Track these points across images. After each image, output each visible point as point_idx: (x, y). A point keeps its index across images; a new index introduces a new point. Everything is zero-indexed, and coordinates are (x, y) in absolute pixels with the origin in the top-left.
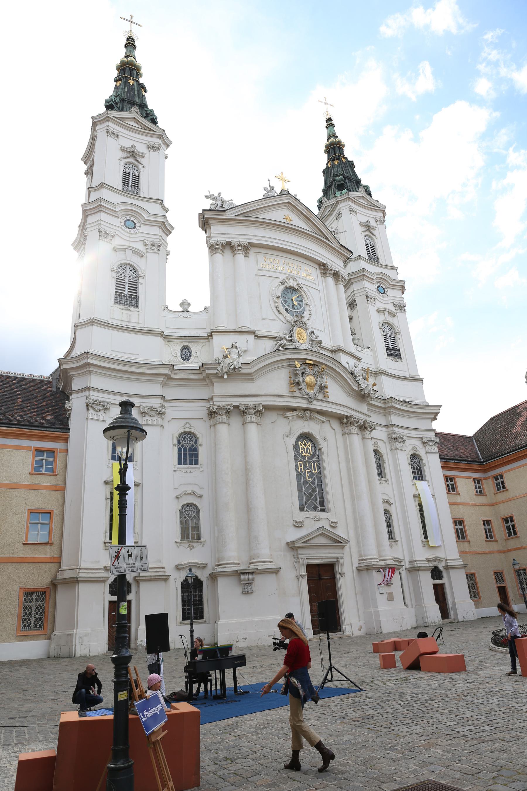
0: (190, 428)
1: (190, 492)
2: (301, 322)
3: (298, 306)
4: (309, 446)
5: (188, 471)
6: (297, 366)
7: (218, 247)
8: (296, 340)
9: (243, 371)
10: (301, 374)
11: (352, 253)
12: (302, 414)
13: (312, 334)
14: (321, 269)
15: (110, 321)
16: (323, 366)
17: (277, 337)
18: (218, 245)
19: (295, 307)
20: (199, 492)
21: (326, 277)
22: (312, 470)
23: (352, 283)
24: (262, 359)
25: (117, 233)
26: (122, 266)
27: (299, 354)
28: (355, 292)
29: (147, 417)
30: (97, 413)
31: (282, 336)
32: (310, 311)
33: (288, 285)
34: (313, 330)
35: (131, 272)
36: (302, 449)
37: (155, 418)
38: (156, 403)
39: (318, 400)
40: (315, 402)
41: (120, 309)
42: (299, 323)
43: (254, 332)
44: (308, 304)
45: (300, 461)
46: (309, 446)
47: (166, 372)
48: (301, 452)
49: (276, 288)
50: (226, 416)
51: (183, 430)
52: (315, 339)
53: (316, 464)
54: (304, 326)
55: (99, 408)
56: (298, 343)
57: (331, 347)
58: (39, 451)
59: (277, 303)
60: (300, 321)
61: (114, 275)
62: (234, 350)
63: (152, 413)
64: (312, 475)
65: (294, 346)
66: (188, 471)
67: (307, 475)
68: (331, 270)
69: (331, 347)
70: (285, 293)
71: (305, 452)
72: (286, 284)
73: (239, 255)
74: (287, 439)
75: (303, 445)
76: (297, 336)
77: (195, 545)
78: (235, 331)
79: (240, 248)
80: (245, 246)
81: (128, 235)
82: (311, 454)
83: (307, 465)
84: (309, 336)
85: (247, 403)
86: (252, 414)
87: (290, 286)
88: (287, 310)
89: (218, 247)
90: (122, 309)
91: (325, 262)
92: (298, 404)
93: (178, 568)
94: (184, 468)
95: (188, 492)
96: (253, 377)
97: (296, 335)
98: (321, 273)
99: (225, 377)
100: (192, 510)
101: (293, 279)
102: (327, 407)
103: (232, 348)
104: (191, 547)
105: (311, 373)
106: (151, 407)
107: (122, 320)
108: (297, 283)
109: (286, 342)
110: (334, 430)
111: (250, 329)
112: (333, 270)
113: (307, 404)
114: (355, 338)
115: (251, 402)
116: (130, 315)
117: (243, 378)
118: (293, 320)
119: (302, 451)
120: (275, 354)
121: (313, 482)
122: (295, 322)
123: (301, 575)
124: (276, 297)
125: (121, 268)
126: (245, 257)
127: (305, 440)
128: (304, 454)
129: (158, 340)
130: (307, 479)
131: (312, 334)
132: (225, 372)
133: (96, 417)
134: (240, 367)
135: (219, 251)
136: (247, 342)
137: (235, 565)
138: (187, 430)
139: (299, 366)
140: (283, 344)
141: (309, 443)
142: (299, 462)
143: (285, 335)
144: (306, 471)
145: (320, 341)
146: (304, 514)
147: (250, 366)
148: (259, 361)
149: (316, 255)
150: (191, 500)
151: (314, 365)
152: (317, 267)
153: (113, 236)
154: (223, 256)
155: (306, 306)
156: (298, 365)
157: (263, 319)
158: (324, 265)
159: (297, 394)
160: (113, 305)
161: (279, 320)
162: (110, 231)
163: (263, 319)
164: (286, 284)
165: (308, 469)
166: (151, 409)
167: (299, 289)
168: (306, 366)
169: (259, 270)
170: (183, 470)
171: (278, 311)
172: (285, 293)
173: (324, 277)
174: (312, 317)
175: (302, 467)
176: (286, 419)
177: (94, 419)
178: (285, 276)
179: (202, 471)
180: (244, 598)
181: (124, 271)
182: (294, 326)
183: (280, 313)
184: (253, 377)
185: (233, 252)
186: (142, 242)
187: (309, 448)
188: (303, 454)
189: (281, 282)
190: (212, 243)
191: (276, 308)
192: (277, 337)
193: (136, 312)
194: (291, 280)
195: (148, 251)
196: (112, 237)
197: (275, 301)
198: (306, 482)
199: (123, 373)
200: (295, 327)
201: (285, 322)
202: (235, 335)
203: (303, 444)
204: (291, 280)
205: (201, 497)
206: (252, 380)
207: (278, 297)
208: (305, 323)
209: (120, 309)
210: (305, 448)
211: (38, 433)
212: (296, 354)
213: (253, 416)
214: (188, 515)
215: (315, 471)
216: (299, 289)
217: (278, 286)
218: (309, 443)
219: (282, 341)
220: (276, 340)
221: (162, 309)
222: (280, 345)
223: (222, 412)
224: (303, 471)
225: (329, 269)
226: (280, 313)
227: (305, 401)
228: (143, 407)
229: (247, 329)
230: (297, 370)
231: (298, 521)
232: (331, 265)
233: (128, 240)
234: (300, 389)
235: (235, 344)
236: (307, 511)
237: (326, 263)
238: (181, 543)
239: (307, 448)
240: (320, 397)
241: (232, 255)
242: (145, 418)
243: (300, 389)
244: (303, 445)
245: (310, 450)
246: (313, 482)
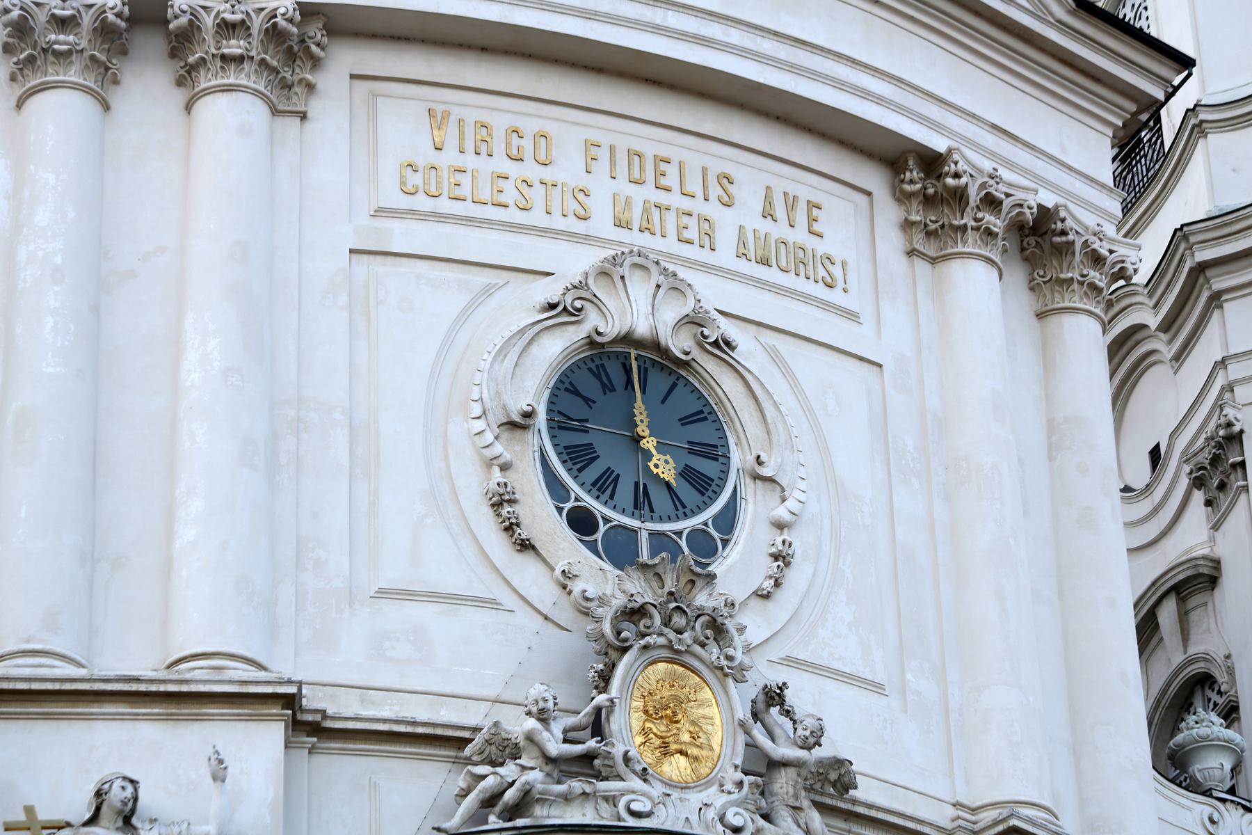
2: (679, 621)
3: (687, 493)
7: (61, 41)
8: (627, 759)
11: (1185, 63)
13: (774, 711)
14: (910, 195)
17: (479, 739)
18: (63, 23)
19: (660, 498)
21: (945, 258)
23: (1216, 299)
28: (1235, 371)
31: (519, 725)
32: (780, 526)
33: (611, 330)
34: (775, 677)
42: (667, 622)
43: (290, 701)
44: (765, 472)
49: (502, 353)
52: (802, 754)
54: (713, 653)
56: (637, 783)
57: (952, 812)
59: (504, 468)
60: (676, 605)
65: (605, 809)
68: (991, 203)
69: (952, 812)
70: (576, 392)
72: (592, 320)
73: (223, 100)
78: (134, 687)
79: (234, 47)
80: (274, 34)
84: (742, 724)
87: (627, 339)
88: (582, 522)
89: (61, 41)
91: (940, 144)
97: (637, 720)
98: (907, 225)
101: (656, 278)
103: (93, 820)
108: (688, 308)
109: (536, 776)
111: (262, 675)
112: (1007, 203)
114: (1206, 738)
118: (619, 601)
122: (635, 613)
124: (497, 417)
126: (275, 112)
131: (774, 711)
135: (73, 76)
140: (510, 795)
143: (532, 723)
145: (839, 763)
149: (864, 94)
152: (873, 178)
154: (106, 107)
155: (749, 490)
157: (385, 593)
158: (932, 163)
161: (509, 600)
163: (385, 593)
164: (592, 320)
167: (696, 353)
169: (380, 212)
171: (509, 529)
172: (576, 392)
173: (933, 261)
174: (796, 578)
178: (592, 257)
182: (624, 650)
183: (526, 546)
185: (187, 77)
189: (552, 306)
190: (16, 13)
191: (497, 506)
192: (479, 739)
194: (640, 289)
197: (489, 453)
200: (627, 658)
201: (565, 615)
202: (136, 717)
204: (640, 289)
207: (518, 425)
208: (718, 629)
216: (696, 353)
217: (529, 337)
219: (509, 771)
220: (469, 761)
222: (490, 801)
225: (974, 196)
226: (526, 546)
229: (236, 676)
232: (987, 165)
235: (118, 794)
237: (950, 151)
241: (178, 97)
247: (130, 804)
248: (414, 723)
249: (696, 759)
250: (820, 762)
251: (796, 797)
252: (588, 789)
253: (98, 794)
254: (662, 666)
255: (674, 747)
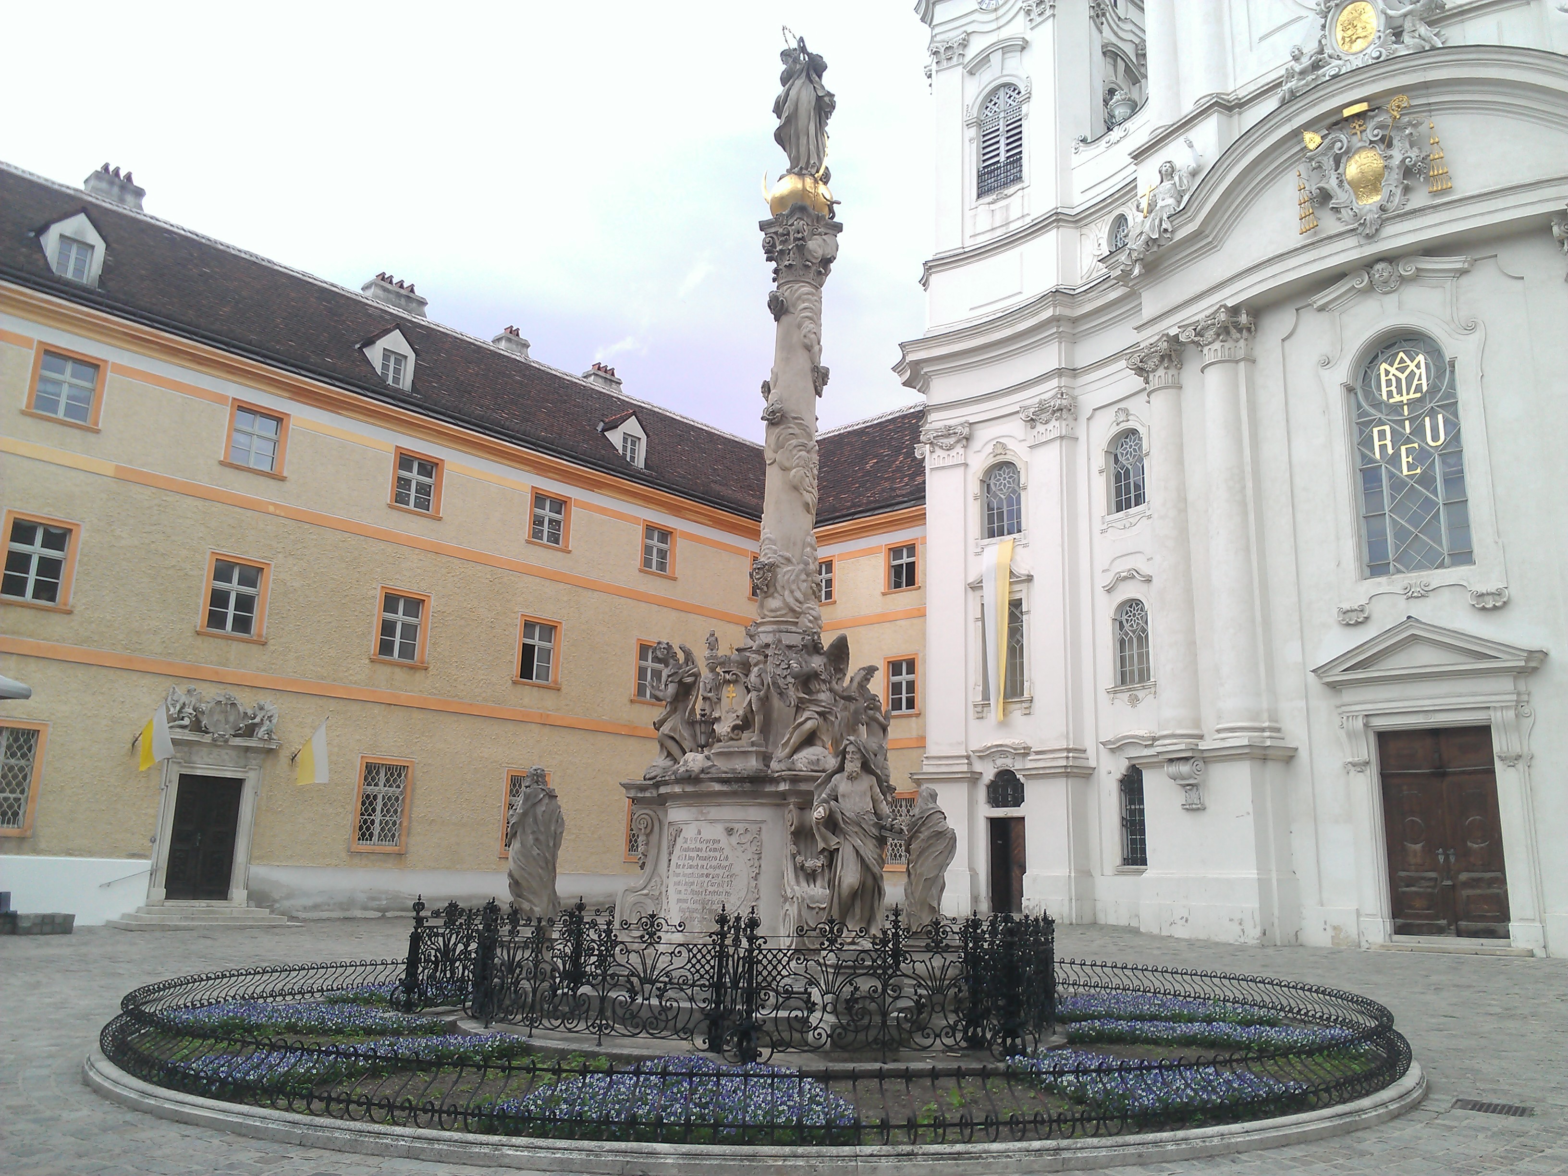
0: (1128, 420)
1: (1125, 574)
4: (1418, 366)
5: (1128, 525)
6: (1312, 146)
8: (1330, 57)
9: (1180, 235)
10: (1332, 162)
12: (1360, 282)
15: (970, 244)
16: (1395, 103)
20: (1145, 569)
22: (1424, 439)
24: (1215, 179)
25: (969, 29)
26: (991, 97)
27: (1314, 105)
29: (1040, 428)
30: (948, 452)
35: (1010, 101)
36: (1389, 383)
37: (1050, 426)
38: (1047, 390)
39: (1398, 216)
40: (1390, 230)
41: (989, 204)
45: (1381, 423)
46: (1418, 366)
47: (1048, 313)
48: (1385, 397)
50: (1167, 368)
51: (1115, 430)
53: (1440, 417)
55: (952, 440)
58: (896, 552)
61: (973, 132)
62: (1167, 184)
63: (1044, 417)
64: (1421, 456)
66: (1128, 525)
67: (1404, 460)
71: (1400, 392)
74: (1325, 373)
75: (1393, 370)
76: (1343, 38)
77: (1141, 694)
81: (993, 16)
82: (1425, 388)
83: (1408, 430)
85: (1196, 318)
86: (1210, 343)
90: (992, 203)
92: (1327, 260)
93: (1116, 747)
94: (1120, 520)
95: (1123, 574)
96: (1210, 239)
99: (1136, 272)
100: (1139, 614)
102: (1441, 224)
103: (1162, 182)
104: (1134, 701)
105: (1360, 145)
106: (1040, 403)
107: (993, 229)
110: (1522, 278)
113: (1361, 246)
115: (1199, 312)
116: (1007, 207)
117: (1189, 251)
119: (1390, 394)
120: (1243, 147)
121: (1426, 480)
123: (1354, 765)
125: (990, 105)
127: (1401, 354)
128: (1397, 398)
129: (1050, 239)
130: (1405, 472)
132: (1136, 261)
133: (949, 462)
134: (1166, 230)
136: (1191, 146)
137: (1175, 741)
138: (1124, 426)
139: (1318, 139)
141: (1421, 358)
142: (1375, 430)
144: (1403, 448)
146: (1381, 583)
147: (1189, 214)
148: (1208, 188)
150: (1129, 591)
151: (1375, 104)
153: (964, 44)
156: (1312, 140)
159: (1330, 224)
160: (974, 205)
162: (955, 36)
165: (1408, 441)
166: (1042, 408)
168: (1341, 130)
170: (1119, 525)
175: (1388, 442)
176: (1324, 314)
177: (943, 468)
179: (1149, 517)
180: (1188, 819)
181: (995, 108)
184: (1210, 239)
186: (1022, 12)
187: (1417, 372)
188: (1391, 401)
193: (1020, 193)
195: (1034, 24)
196: (961, 47)
198: (1397, 484)
199: (972, 354)
203: (1396, 365)
205: (1148, 580)
206: (1212, 247)
209: (989, 204)
210: (1403, 377)
211: (885, 518)
212: (1306, 110)
213: (1217, 345)
214: (1132, 626)
215: (1435, 438)
218: (1421, 358)
221: (1074, 151)
223: (1150, 365)
224: (1390, 451)
227: (1351, 241)
228: (1026, 408)
230: (1311, 159)
231: (1346, 606)
233: (995, 27)
234: (1336, 210)
236: (1399, 571)
238: (1115, 692)
239: (1411, 376)
240: (1419, 199)
242: (1035, 432)
243: (1336, 210)
244: (1393, 370)
245: (1420, 379)
246: (1426, 480)
247: (1170, 169)
248: (1268, 84)
249: (1365, 37)
250: (1423, 5)
251: (1414, 26)
252: (1314, 77)
253: (1160, 172)
254: (1350, 7)
255: (1354, 37)
